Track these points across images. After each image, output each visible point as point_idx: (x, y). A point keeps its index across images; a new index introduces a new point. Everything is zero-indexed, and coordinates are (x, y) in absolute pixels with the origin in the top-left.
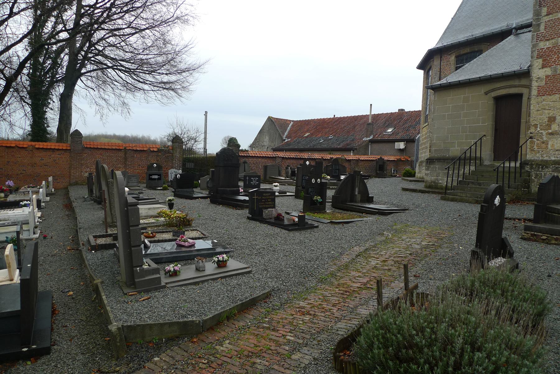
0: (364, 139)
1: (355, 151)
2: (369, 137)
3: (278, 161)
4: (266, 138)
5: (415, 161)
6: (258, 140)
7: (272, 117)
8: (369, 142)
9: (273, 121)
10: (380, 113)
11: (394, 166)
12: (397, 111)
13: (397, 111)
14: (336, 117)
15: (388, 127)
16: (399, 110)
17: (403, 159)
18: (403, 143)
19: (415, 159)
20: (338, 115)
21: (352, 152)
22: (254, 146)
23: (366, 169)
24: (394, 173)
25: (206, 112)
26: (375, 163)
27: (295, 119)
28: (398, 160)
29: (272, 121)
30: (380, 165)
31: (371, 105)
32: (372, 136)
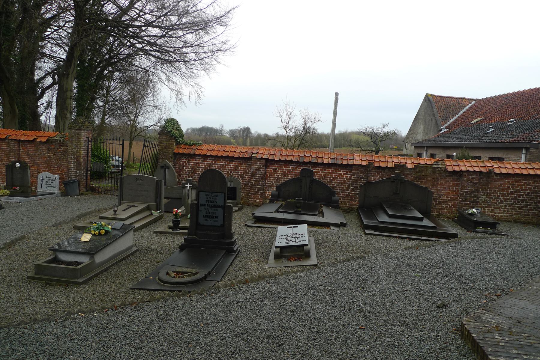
1: (532, 150)
3: (257, 166)
4: (420, 128)
6: (412, 132)
7: (431, 95)
9: (431, 100)
21: (524, 152)
22: (408, 140)
23: (515, 199)
25: (337, 94)
27: (480, 97)
29: (429, 100)
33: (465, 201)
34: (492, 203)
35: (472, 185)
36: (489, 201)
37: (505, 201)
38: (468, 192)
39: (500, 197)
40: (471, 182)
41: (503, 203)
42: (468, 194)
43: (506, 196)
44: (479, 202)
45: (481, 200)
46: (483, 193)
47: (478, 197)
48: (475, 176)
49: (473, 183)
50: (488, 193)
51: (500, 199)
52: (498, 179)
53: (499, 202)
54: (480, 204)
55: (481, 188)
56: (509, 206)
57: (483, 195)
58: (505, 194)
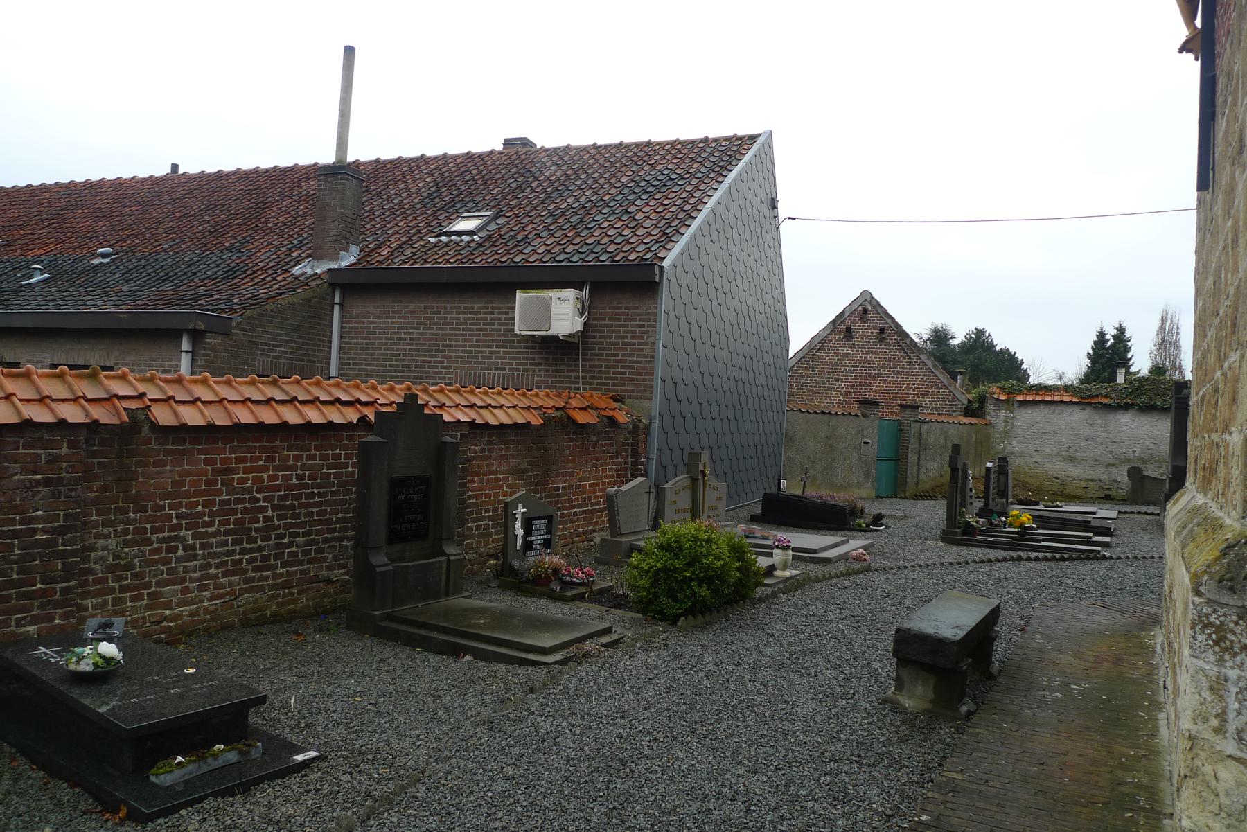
0: (296, 271)
1: (211, 340)
2: (336, 258)
5: (656, 428)
8: (333, 286)
10: (407, 154)
11: (521, 473)
12: (500, 148)
13: (500, 148)
14: (181, 171)
15: (456, 208)
16: (508, 143)
17: (581, 418)
18: (570, 294)
19: (655, 412)
20: (190, 167)
21: (186, 345)
23: (240, 533)
24: (528, 546)
26: (346, 457)
28: (548, 420)
30: (397, 484)
31: (349, 52)
32: (354, 250)
33: (22, 584)
34: (149, 563)
35: (56, 495)
36: (136, 556)
37: (203, 546)
38: (35, 531)
39: (183, 533)
40: (47, 482)
41: (195, 557)
42: (38, 544)
43: (205, 524)
44: (90, 571)
45: (103, 559)
46: (105, 524)
47: (84, 549)
48: (65, 450)
49: (59, 482)
50: (128, 522)
51: (182, 540)
52: (167, 452)
53: (180, 553)
54: (98, 581)
55: (95, 502)
56: (218, 566)
57: (107, 537)
58: (201, 514)
